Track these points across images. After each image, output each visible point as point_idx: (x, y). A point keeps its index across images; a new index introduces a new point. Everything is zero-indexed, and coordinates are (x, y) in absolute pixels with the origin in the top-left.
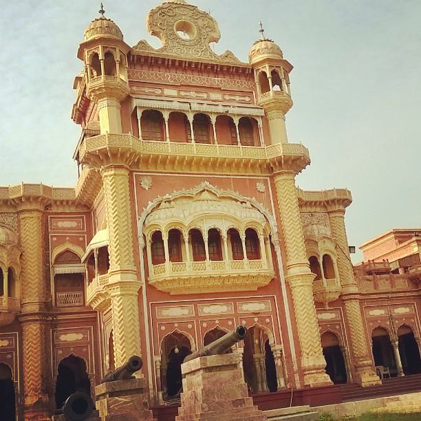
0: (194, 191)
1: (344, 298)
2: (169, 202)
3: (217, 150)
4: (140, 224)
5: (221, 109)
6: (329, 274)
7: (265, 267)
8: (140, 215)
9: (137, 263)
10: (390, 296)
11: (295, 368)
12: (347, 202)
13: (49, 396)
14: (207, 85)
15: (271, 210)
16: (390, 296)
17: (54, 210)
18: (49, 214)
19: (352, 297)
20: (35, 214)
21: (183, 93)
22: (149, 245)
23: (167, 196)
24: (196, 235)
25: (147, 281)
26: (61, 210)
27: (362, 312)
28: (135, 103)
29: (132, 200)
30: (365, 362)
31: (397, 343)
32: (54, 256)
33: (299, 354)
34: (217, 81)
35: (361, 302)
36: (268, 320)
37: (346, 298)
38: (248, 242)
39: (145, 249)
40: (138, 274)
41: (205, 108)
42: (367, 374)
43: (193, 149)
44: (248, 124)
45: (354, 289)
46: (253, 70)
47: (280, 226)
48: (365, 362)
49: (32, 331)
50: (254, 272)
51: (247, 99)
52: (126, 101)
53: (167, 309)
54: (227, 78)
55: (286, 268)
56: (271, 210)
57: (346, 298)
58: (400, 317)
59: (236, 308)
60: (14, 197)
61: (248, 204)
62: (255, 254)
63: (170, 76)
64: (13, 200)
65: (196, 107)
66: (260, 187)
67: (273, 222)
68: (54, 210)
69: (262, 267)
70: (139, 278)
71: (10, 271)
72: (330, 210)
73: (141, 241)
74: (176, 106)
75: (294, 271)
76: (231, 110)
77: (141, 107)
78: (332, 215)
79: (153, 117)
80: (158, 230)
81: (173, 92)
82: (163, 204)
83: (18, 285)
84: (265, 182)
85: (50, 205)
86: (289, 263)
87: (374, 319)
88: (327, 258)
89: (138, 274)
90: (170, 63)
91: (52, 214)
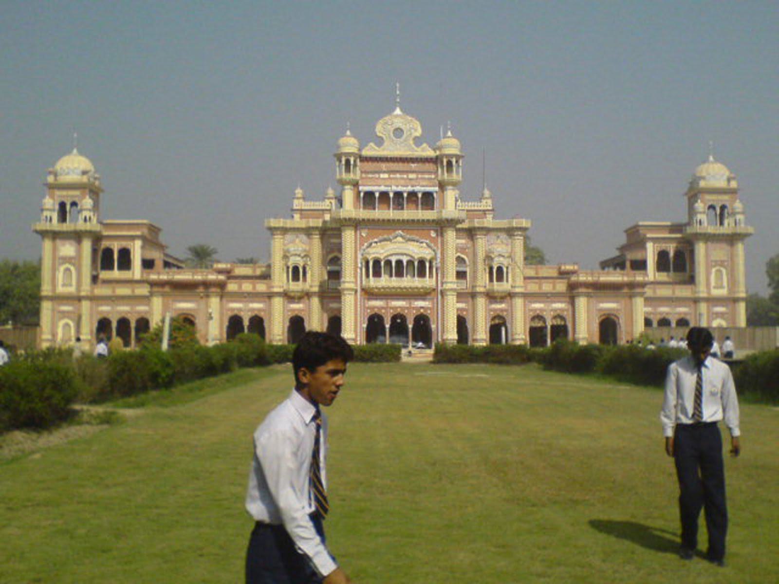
2: (376, 242)
4: (359, 256)
6: (500, 278)
7: (428, 283)
9: (356, 277)
23: (376, 240)
24: (388, 263)
28: (361, 188)
29: (356, 242)
33: (443, 332)
34: (413, 166)
38: (421, 268)
39: (361, 269)
40: (356, 283)
41: (400, 189)
43: (391, 214)
44: (428, 196)
47: (443, 259)
50: (420, 286)
54: (420, 165)
55: (442, 283)
61: (424, 245)
62: (422, 274)
63: (384, 166)
65: (395, 188)
66: (433, 234)
67: (439, 255)
71: (304, 269)
79: (369, 195)
81: (386, 176)
82: (374, 245)
83: (308, 275)
84: (436, 231)
86: (445, 280)
88: (500, 269)
89: (356, 283)
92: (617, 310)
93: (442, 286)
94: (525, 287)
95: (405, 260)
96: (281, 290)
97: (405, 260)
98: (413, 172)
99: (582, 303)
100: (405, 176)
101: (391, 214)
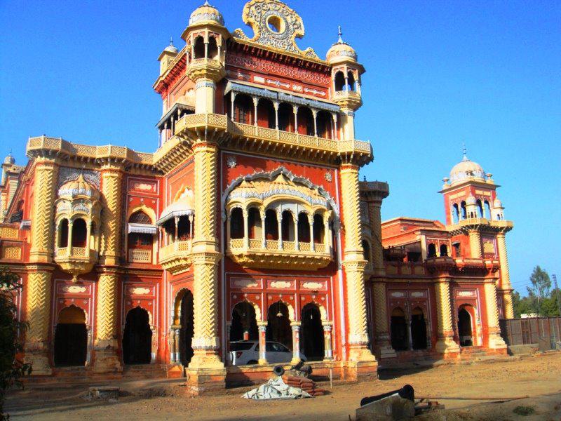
0: (270, 173)
1: (374, 280)
2: (248, 181)
3: (294, 138)
5: (304, 102)
8: (224, 191)
10: (410, 281)
11: (343, 342)
12: (385, 194)
13: (118, 342)
14: (291, 76)
15: (335, 199)
16: (410, 281)
17: (132, 172)
18: (129, 175)
19: (381, 280)
20: (116, 175)
21: (269, 82)
22: (229, 219)
25: (225, 253)
26: (138, 173)
27: (386, 293)
30: (385, 337)
31: (411, 322)
32: (127, 218)
33: (347, 331)
35: (387, 284)
36: (323, 299)
37: (375, 280)
38: (311, 228)
39: (225, 224)
41: (290, 99)
42: (385, 347)
45: (382, 273)
46: (331, 68)
48: (385, 337)
49: (105, 283)
51: (323, 94)
52: (220, 84)
53: (239, 280)
56: (335, 199)
57: (375, 280)
58: (414, 300)
59: (298, 285)
60: (100, 156)
64: (100, 159)
68: (132, 172)
69: (322, 250)
70: (220, 251)
72: (370, 199)
73: (223, 216)
74: (266, 93)
75: (348, 258)
76: (312, 104)
77: (235, 91)
78: (371, 205)
79: (244, 101)
80: (239, 207)
81: (262, 80)
82: (244, 183)
85: (130, 168)
86: (346, 250)
87: (395, 300)
90: (262, 53)
91: (131, 175)
92: (474, 300)
93: (343, 259)
94: (385, 270)
95: (296, 210)
96: (45, 259)
97: (296, 210)
98: (299, 82)
99: (444, 289)
100: (288, 86)
101: (276, 135)
